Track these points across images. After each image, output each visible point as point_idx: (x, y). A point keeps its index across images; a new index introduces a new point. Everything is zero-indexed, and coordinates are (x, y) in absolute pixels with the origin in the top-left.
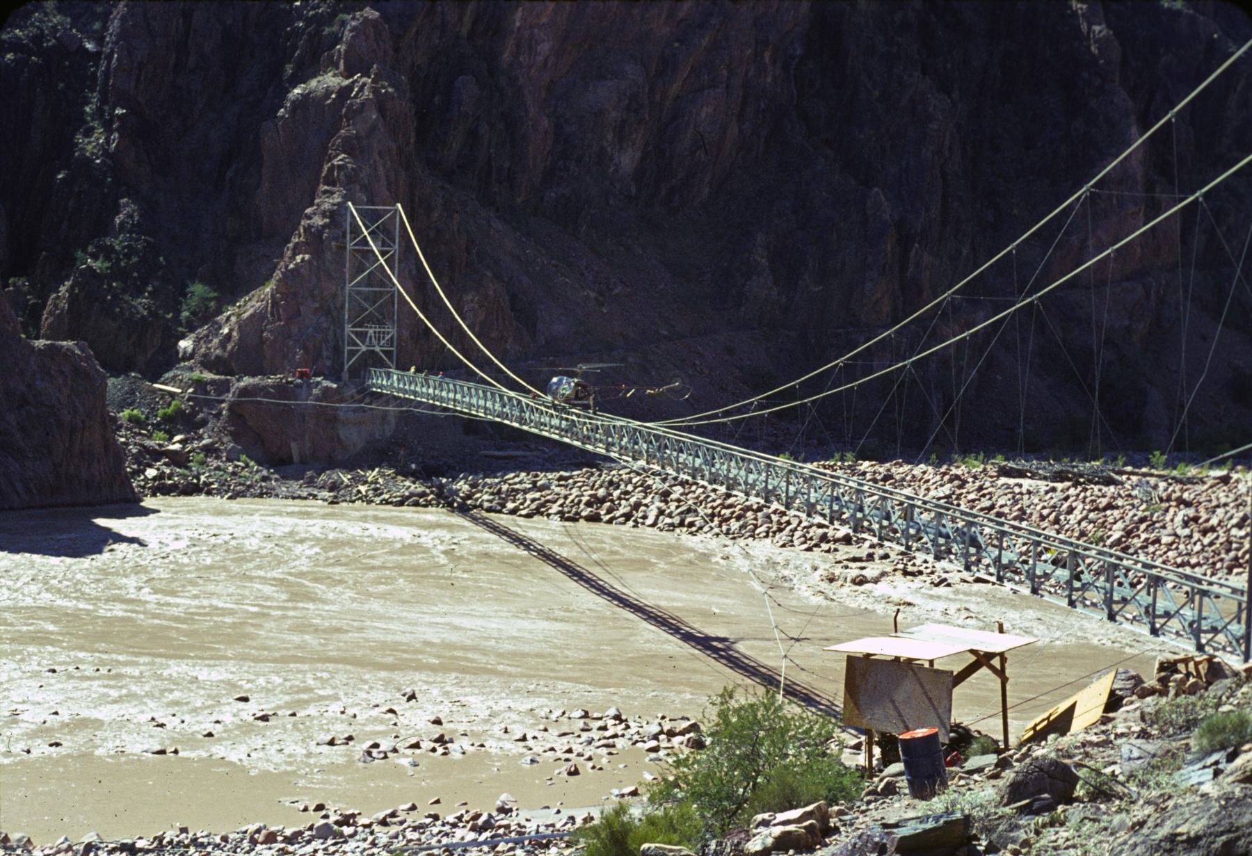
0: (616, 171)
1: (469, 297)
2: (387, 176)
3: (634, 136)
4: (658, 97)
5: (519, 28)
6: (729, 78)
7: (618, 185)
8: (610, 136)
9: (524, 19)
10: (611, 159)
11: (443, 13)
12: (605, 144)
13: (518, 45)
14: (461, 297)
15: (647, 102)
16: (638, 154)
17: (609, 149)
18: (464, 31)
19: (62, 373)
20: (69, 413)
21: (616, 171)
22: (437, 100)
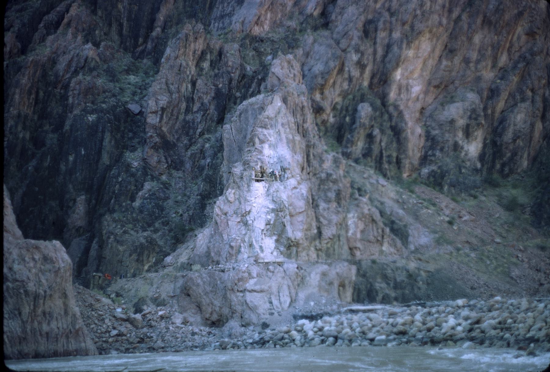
0: (466, 155)
1: (350, 215)
2: (287, 138)
3: (476, 134)
4: (489, 112)
5: (400, 80)
6: (533, 97)
7: (468, 164)
8: (460, 134)
9: (402, 75)
10: (462, 148)
11: (349, 71)
12: (457, 139)
13: (400, 89)
14: (346, 216)
15: (482, 114)
16: (480, 145)
17: (460, 142)
18: (366, 84)
19: (34, 259)
20: (35, 285)
21: (466, 155)
22: (347, 119)
